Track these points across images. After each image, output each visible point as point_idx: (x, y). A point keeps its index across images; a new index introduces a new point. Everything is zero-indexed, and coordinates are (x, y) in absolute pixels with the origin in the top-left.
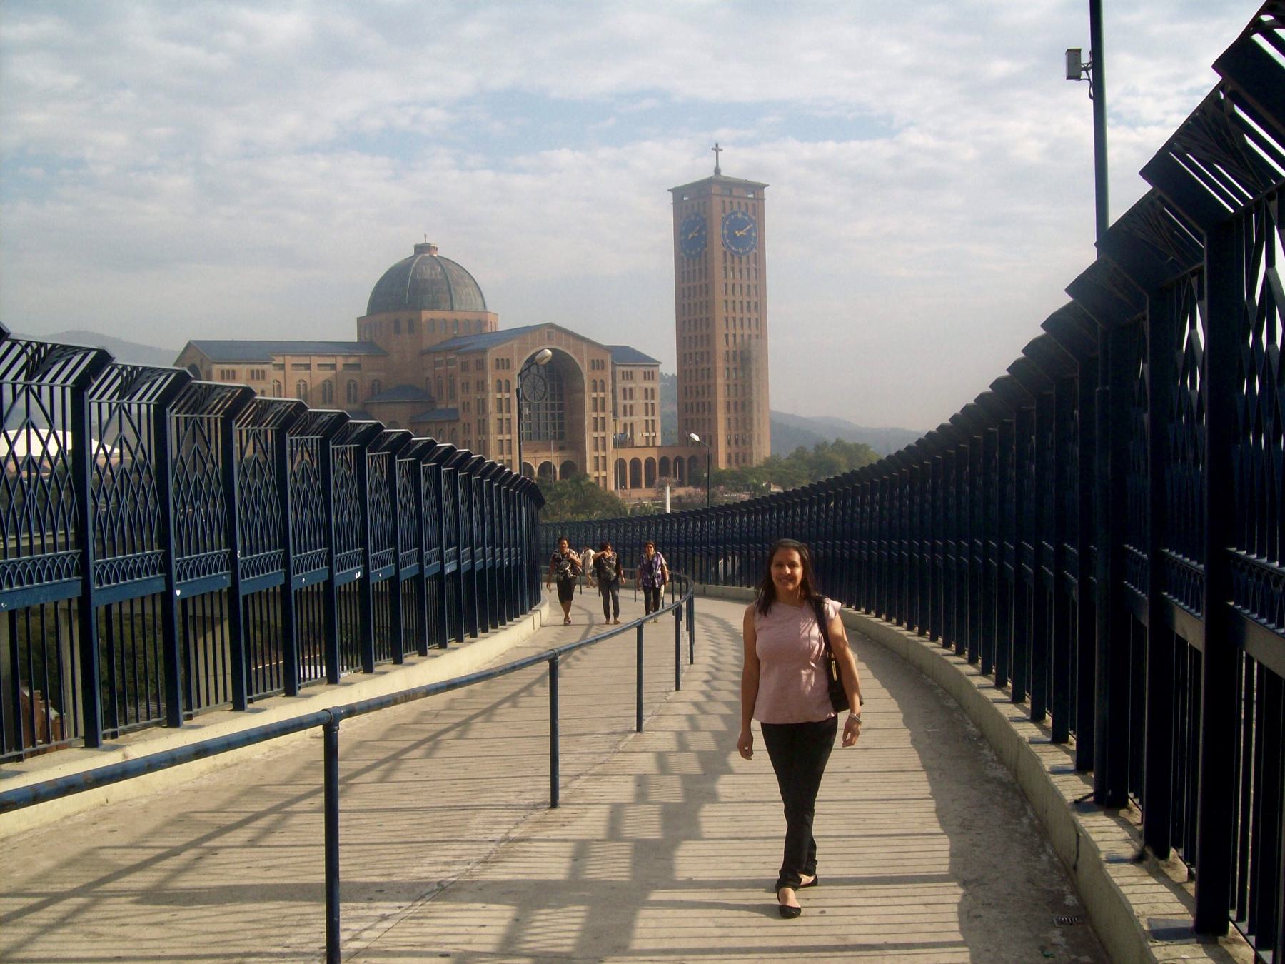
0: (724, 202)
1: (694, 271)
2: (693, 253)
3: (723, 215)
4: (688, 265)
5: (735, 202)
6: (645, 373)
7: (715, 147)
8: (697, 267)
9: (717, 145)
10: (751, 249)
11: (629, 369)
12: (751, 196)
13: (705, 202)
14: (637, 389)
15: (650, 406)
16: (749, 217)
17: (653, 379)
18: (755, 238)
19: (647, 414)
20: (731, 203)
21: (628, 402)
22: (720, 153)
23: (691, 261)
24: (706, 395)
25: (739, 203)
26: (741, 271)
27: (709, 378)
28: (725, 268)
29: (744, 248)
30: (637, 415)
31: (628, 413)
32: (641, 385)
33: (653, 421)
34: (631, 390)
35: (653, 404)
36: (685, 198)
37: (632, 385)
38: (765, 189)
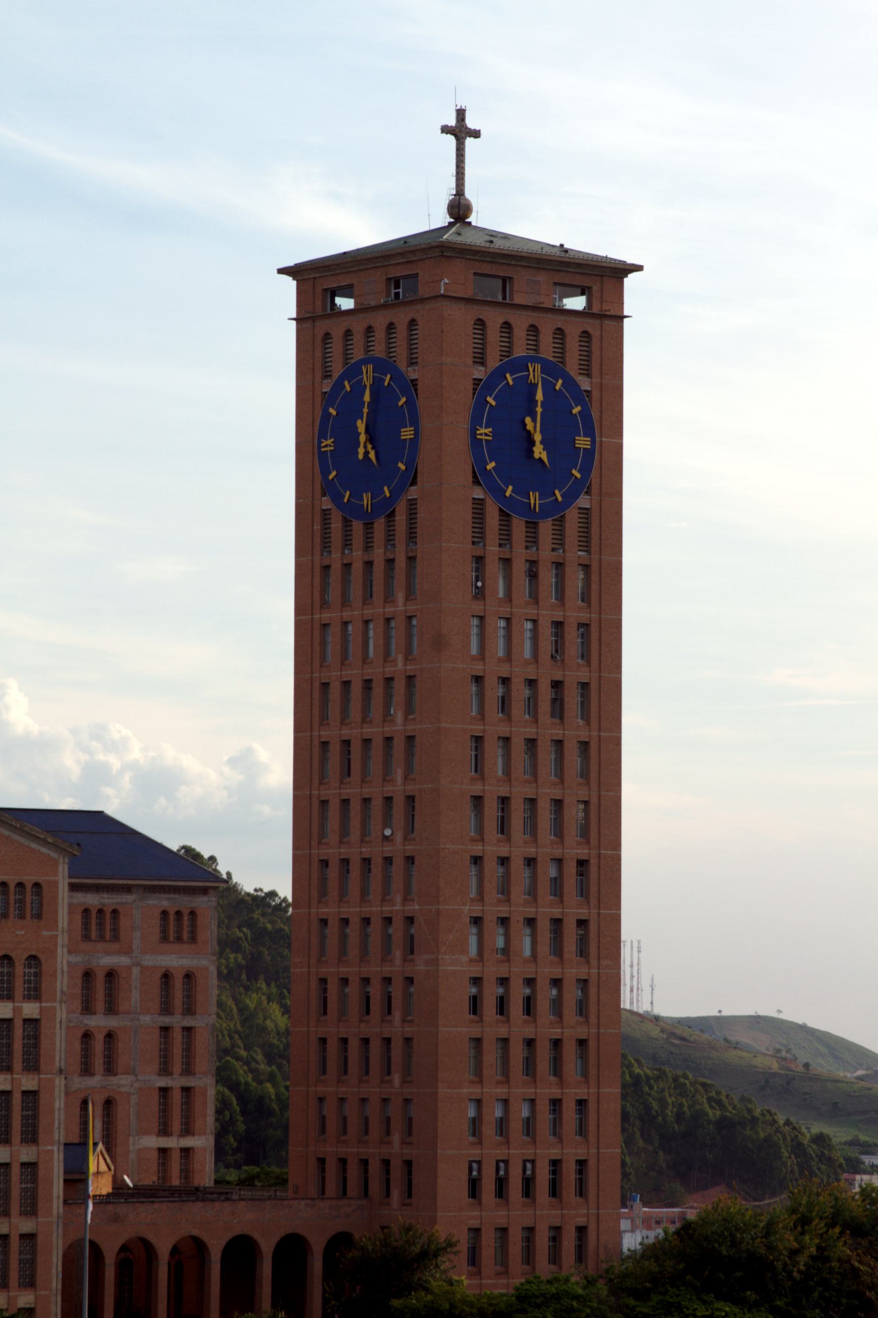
0: (480, 323)
1: (369, 564)
2: (366, 499)
3: (480, 373)
4: (347, 543)
5: (521, 322)
6: (164, 913)
7: (452, 122)
8: (378, 554)
9: (461, 114)
10: (570, 497)
11: (108, 900)
12: (576, 303)
13: (413, 323)
14: (136, 971)
15: (177, 1037)
16: (570, 383)
17: (193, 939)
18: (589, 454)
19: (165, 1070)
20: (507, 326)
21: (99, 1022)
22: (469, 142)
23: (358, 526)
24: (397, 1015)
25: (534, 330)
26: (533, 575)
27: (410, 947)
28: (479, 560)
29: (546, 492)
30: (131, 1071)
31: (99, 1062)
32: (149, 960)
33: (186, 1090)
34: (111, 975)
35: (188, 1030)
36: (345, 303)
37: (124, 960)
38: (630, 282)
